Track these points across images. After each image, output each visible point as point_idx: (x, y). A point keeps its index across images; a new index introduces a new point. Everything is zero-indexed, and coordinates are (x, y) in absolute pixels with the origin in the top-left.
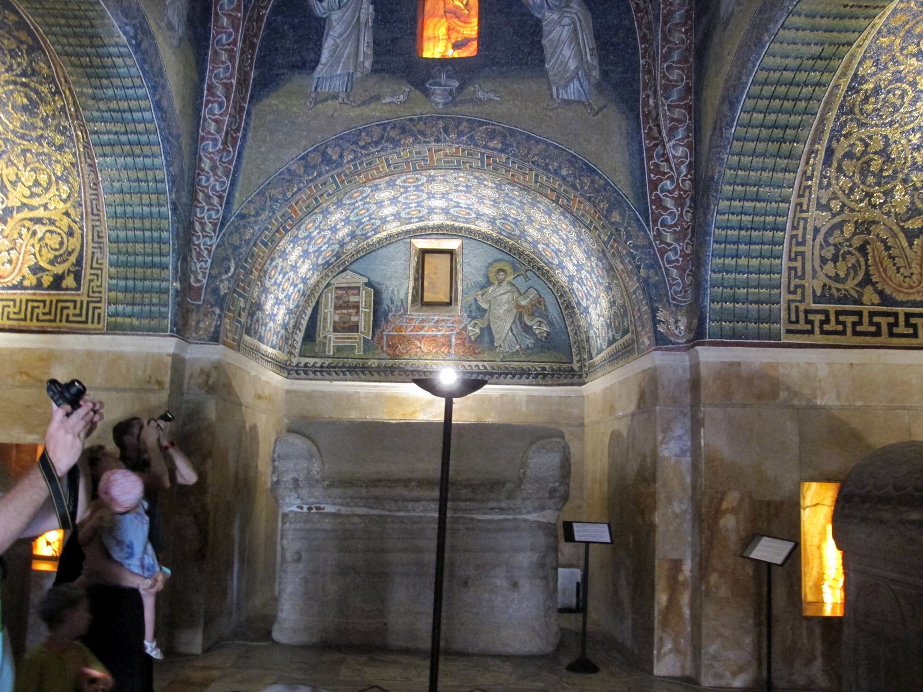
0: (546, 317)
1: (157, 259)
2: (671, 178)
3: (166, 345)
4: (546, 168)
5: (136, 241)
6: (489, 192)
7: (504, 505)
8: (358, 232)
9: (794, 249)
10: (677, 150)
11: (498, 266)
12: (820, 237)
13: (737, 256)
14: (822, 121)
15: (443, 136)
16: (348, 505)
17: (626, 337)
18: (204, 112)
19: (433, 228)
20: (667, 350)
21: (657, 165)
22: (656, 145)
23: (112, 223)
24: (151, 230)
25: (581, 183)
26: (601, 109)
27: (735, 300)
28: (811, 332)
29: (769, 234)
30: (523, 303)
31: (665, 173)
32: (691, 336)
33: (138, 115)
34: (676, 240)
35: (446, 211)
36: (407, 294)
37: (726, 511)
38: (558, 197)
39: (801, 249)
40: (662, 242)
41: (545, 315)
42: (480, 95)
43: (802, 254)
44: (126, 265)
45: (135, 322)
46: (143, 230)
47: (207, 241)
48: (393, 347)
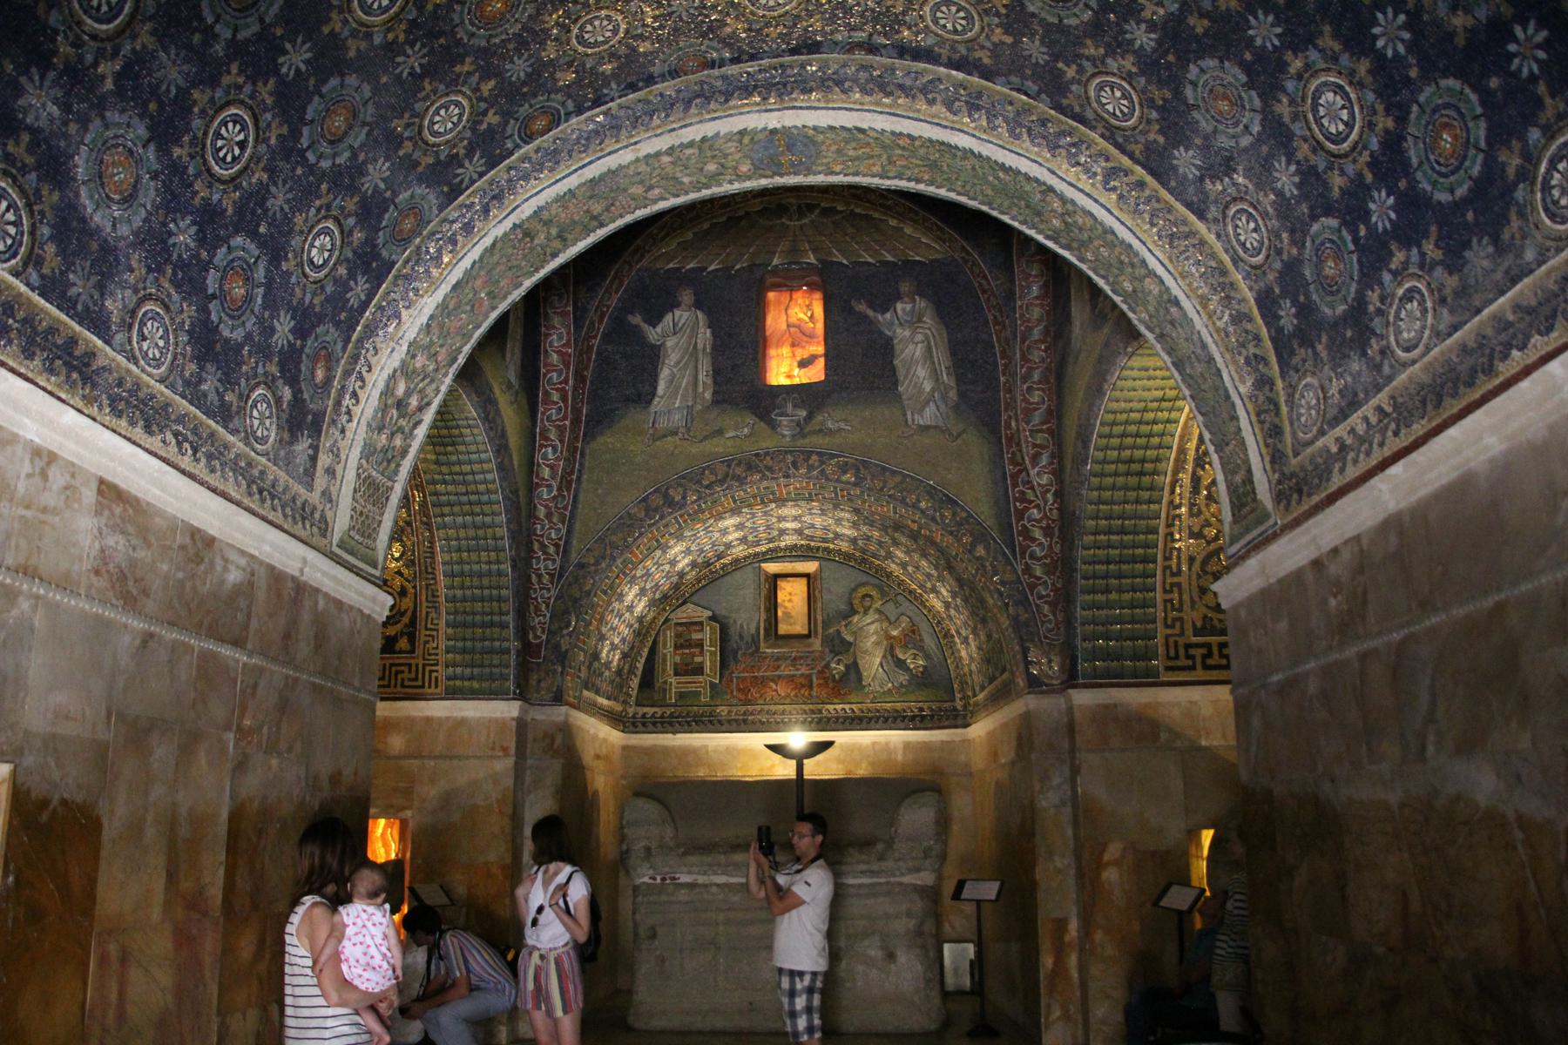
0: (921, 648)
1: (496, 618)
2: (1038, 507)
3: (507, 710)
4: (903, 501)
5: (474, 599)
6: (847, 515)
7: (875, 867)
8: (700, 560)
9: (1169, 581)
10: (1041, 477)
11: (862, 591)
12: (1197, 566)
13: (1107, 591)
14: (1182, 451)
15: (792, 471)
16: (705, 874)
17: (1005, 676)
18: (539, 458)
19: (787, 548)
20: (1042, 692)
21: (1023, 493)
22: (1020, 471)
23: (448, 581)
24: (490, 587)
25: (942, 516)
26: (959, 435)
27: (1107, 638)
28: (1193, 668)
29: (1139, 567)
30: (895, 633)
31: (1031, 502)
32: (1065, 677)
33: (479, 477)
34: (1048, 573)
35: (799, 532)
36: (758, 629)
37: (1108, 864)
38: (920, 528)
39: (1176, 580)
40: (1031, 576)
41: (920, 647)
42: (830, 425)
43: (1179, 585)
44: (464, 625)
45: (476, 685)
46: (481, 588)
47: (545, 595)
48: (745, 691)
